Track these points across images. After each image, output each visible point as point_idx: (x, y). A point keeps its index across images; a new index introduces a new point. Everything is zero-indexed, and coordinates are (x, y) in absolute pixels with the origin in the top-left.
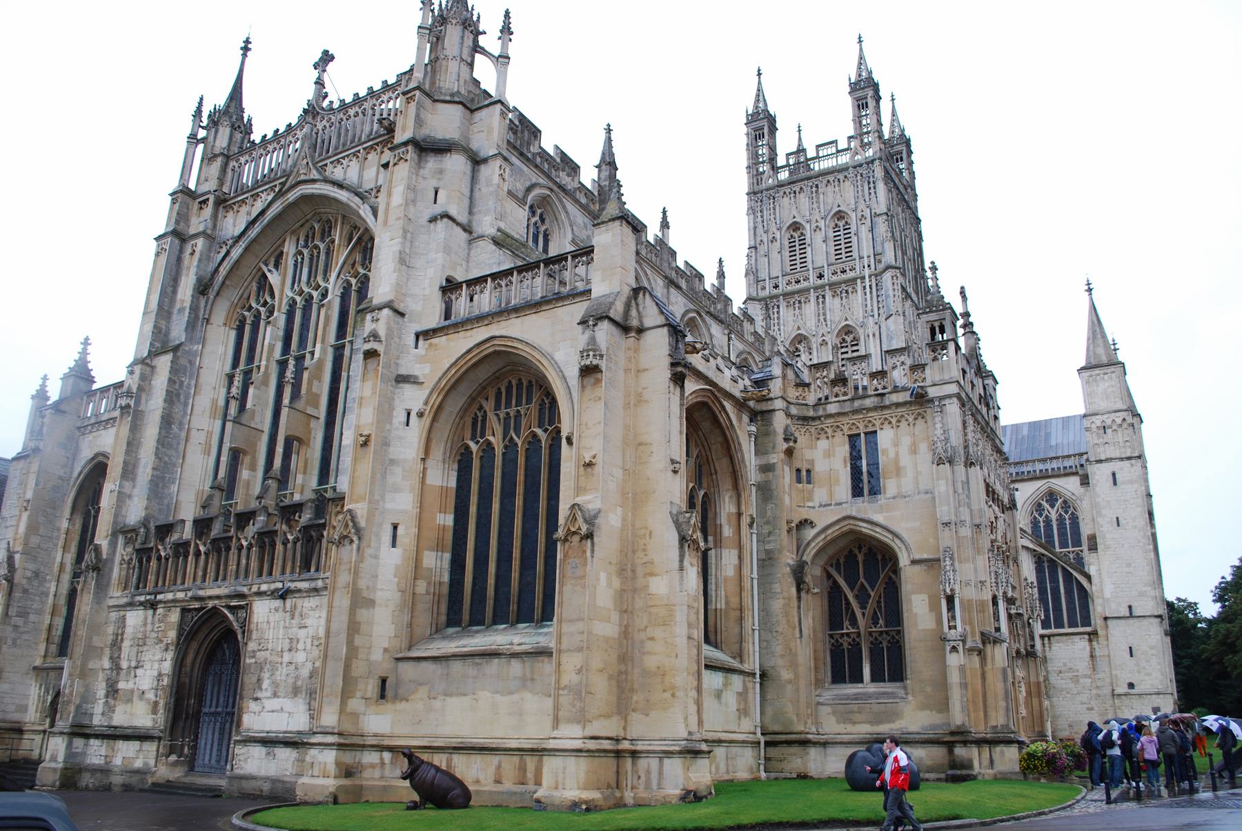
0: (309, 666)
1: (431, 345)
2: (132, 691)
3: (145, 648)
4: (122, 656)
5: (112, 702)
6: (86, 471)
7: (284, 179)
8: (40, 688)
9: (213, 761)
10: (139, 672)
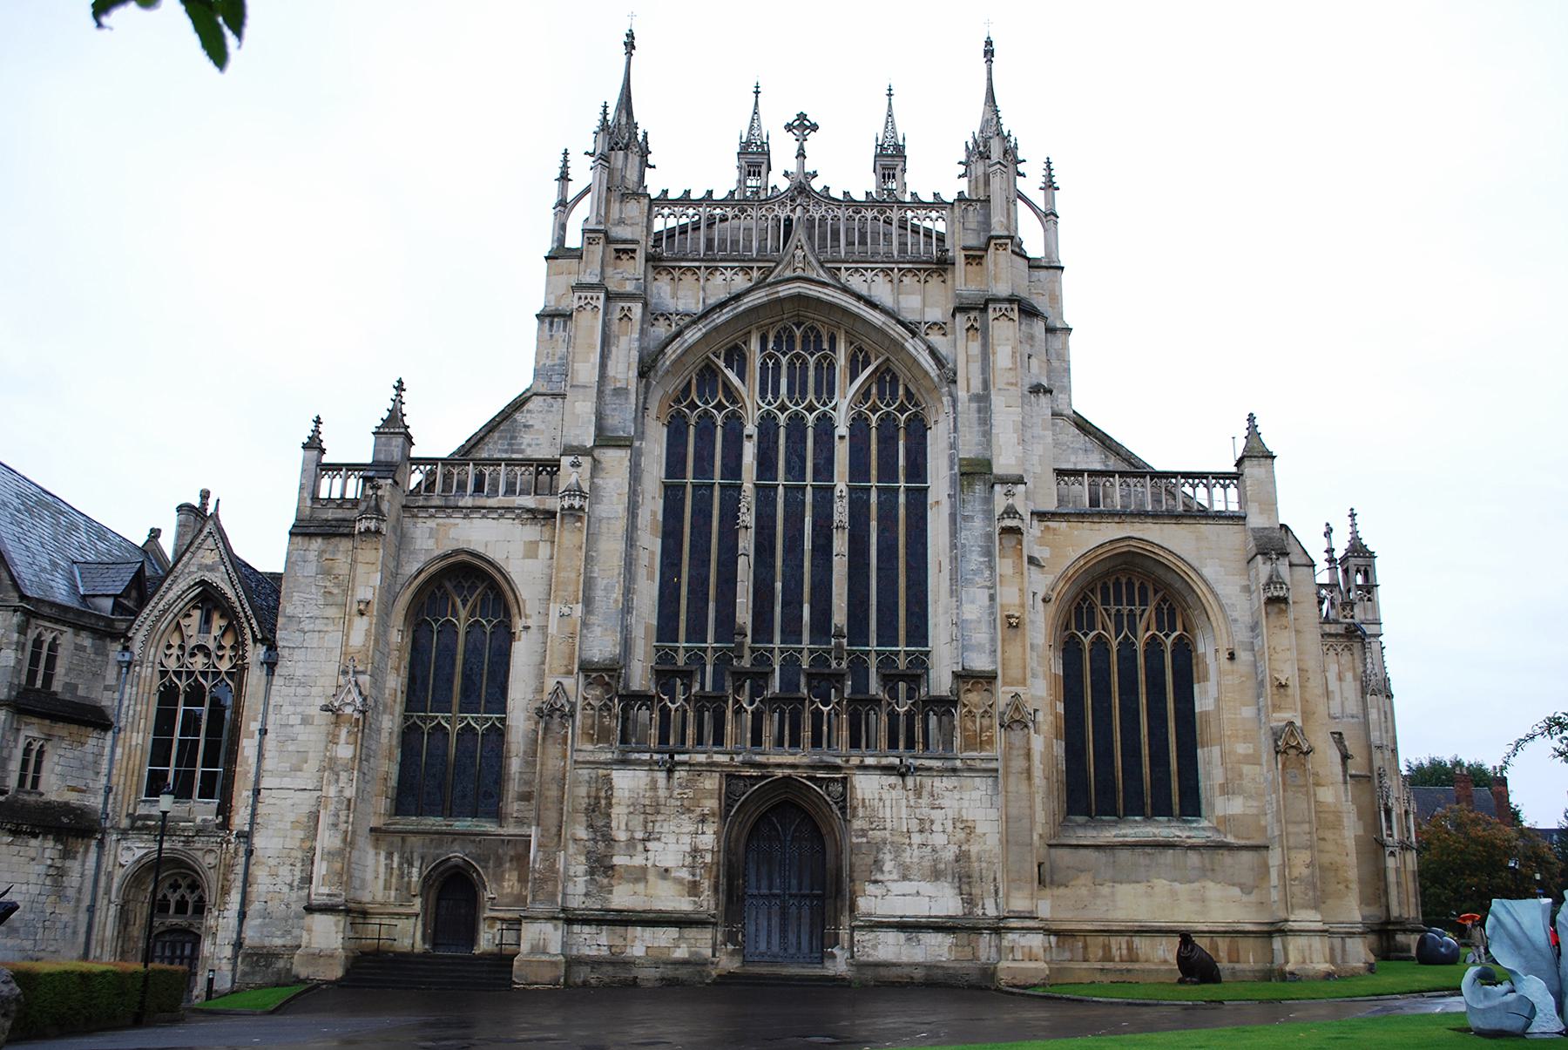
0: (954, 849)
1: (1047, 528)
2: (644, 869)
3: (660, 818)
4: (614, 824)
5: (606, 881)
6: (433, 569)
7: (773, 264)
8: (390, 856)
9: (775, 949)
10: (650, 845)
